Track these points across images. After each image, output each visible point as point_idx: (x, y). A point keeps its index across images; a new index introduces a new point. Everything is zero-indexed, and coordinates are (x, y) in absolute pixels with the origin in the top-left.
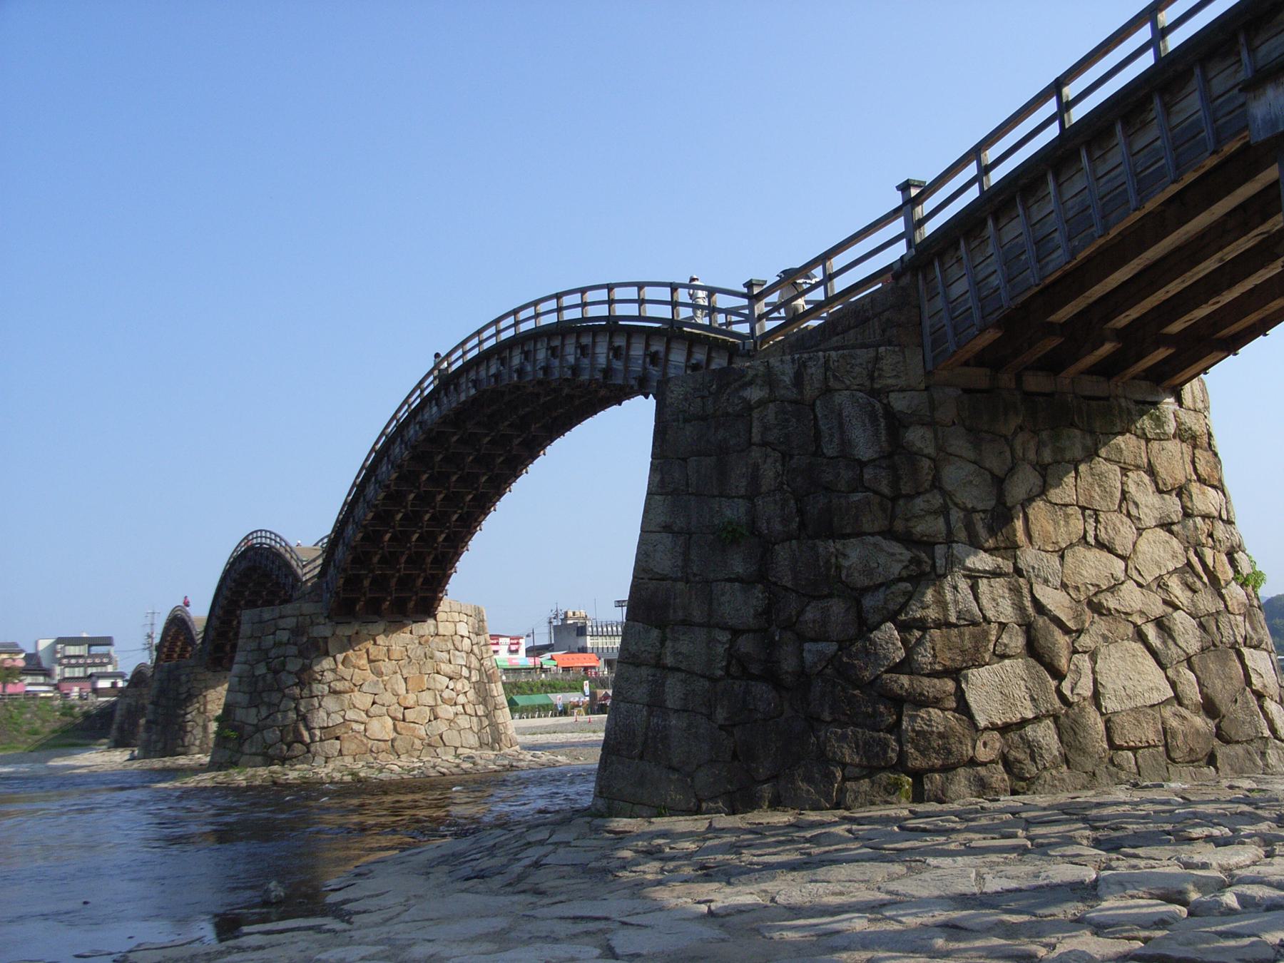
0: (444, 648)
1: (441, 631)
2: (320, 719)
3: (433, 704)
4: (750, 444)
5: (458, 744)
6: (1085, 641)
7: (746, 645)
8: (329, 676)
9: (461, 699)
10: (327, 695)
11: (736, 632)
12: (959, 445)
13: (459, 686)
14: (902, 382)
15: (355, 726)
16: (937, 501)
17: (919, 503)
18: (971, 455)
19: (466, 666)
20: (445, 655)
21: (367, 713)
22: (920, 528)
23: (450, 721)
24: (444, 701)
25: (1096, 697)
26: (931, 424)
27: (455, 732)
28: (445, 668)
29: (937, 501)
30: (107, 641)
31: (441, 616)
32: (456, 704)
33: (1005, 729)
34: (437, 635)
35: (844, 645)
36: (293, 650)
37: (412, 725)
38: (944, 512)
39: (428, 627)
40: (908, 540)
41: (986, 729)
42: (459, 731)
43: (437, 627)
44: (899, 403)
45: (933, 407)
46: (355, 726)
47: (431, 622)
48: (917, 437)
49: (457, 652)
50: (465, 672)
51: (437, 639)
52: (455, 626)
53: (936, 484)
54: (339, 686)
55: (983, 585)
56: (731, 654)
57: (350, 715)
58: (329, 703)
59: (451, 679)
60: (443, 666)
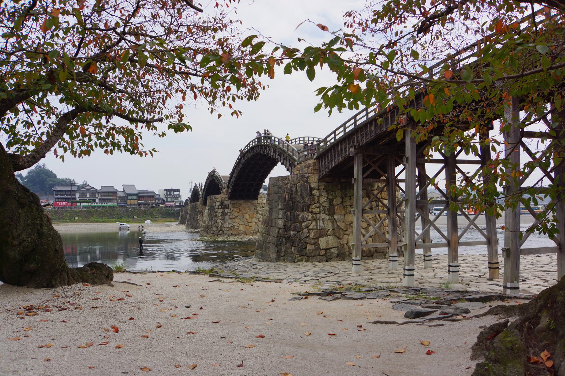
2: (227, 225)
4: (285, 192)
6: (347, 233)
7: (281, 231)
8: (229, 214)
11: (280, 228)
12: (324, 194)
14: (313, 181)
15: (236, 227)
16: (318, 205)
17: (313, 206)
18: (326, 196)
20: (260, 209)
21: (238, 223)
22: (314, 211)
25: (347, 244)
26: (319, 190)
29: (318, 205)
30: (178, 190)
31: (259, 198)
33: (326, 249)
35: (298, 232)
36: (220, 207)
38: (319, 207)
39: (256, 201)
40: (312, 213)
41: (323, 249)
44: (313, 185)
45: (319, 186)
46: (236, 227)
47: (256, 200)
48: (315, 192)
53: (318, 202)
54: (231, 217)
55: (325, 222)
56: (278, 233)
57: (235, 224)
58: (229, 221)
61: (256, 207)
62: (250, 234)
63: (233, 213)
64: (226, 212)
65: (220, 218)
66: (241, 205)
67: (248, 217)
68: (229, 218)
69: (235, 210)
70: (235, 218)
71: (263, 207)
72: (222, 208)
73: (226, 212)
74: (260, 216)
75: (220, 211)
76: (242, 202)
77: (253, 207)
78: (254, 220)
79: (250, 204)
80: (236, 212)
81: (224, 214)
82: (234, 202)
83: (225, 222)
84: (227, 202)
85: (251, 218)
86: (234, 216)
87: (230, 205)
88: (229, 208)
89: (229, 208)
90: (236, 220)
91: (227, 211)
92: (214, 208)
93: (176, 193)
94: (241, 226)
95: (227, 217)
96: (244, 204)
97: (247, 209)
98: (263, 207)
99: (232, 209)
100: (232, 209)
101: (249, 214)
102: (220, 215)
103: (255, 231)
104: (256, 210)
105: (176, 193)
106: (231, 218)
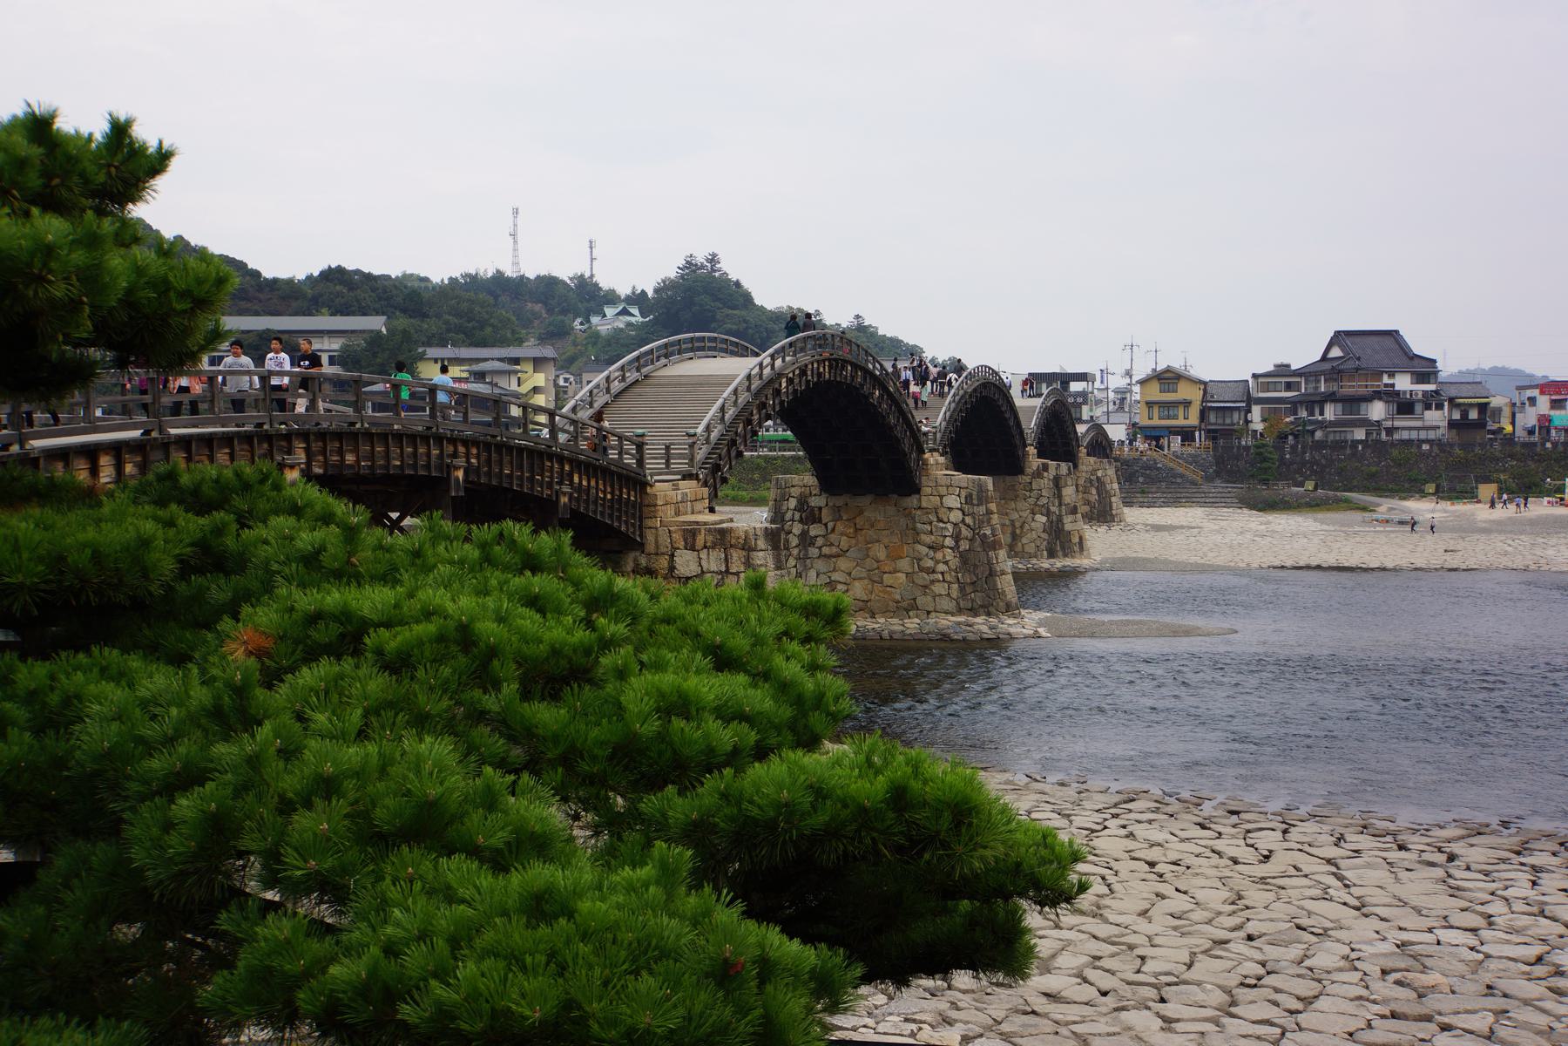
0: (925, 519)
1: (924, 504)
3: (910, 571)
5: (932, 609)
8: (820, 541)
9: (941, 567)
10: (819, 557)
13: (939, 555)
19: (951, 536)
21: (850, 574)
23: (926, 587)
24: (922, 569)
27: (929, 598)
28: (923, 537)
30: (1082, 377)
32: (934, 572)
34: (920, 508)
37: (888, 589)
39: (912, 501)
42: (934, 598)
43: (920, 500)
49: (941, 525)
50: (949, 542)
51: (919, 512)
52: (941, 499)
54: (826, 550)
57: (836, 576)
58: (820, 565)
59: (930, 547)
60: (923, 537)
61: (913, 518)
62: (885, 612)
63: (833, 537)
64: (812, 533)
65: (795, 552)
66: (861, 513)
67: (882, 555)
68: (820, 556)
69: (840, 527)
70: (838, 556)
71: (941, 521)
72: (801, 521)
73: (812, 533)
74: (924, 550)
75: (797, 529)
76: (864, 501)
77: (903, 521)
78: (904, 564)
79: (891, 510)
80: (842, 534)
81: (806, 540)
82: (839, 501)
83: (806, 569)
84: (816, 501)
85: (894, 556)
86: (834, 550)
87: (824, 511)
88: (820, 521)
89: (820, 521)
90: (843, 564)
91: (815, 530)
92: (783, 520)
93: (1075, 387)
94: (857, 584)
95: (813, 552)
96: (876, 512)
97: (882, 525)
98: (941, 521)
99: (830, 525)
100: (830, 525)
101: (886, 541)
102: (794, 541)
103: (905, 604)
104: (914, 529)
105: (1075, 387)
106: (825, 556)
